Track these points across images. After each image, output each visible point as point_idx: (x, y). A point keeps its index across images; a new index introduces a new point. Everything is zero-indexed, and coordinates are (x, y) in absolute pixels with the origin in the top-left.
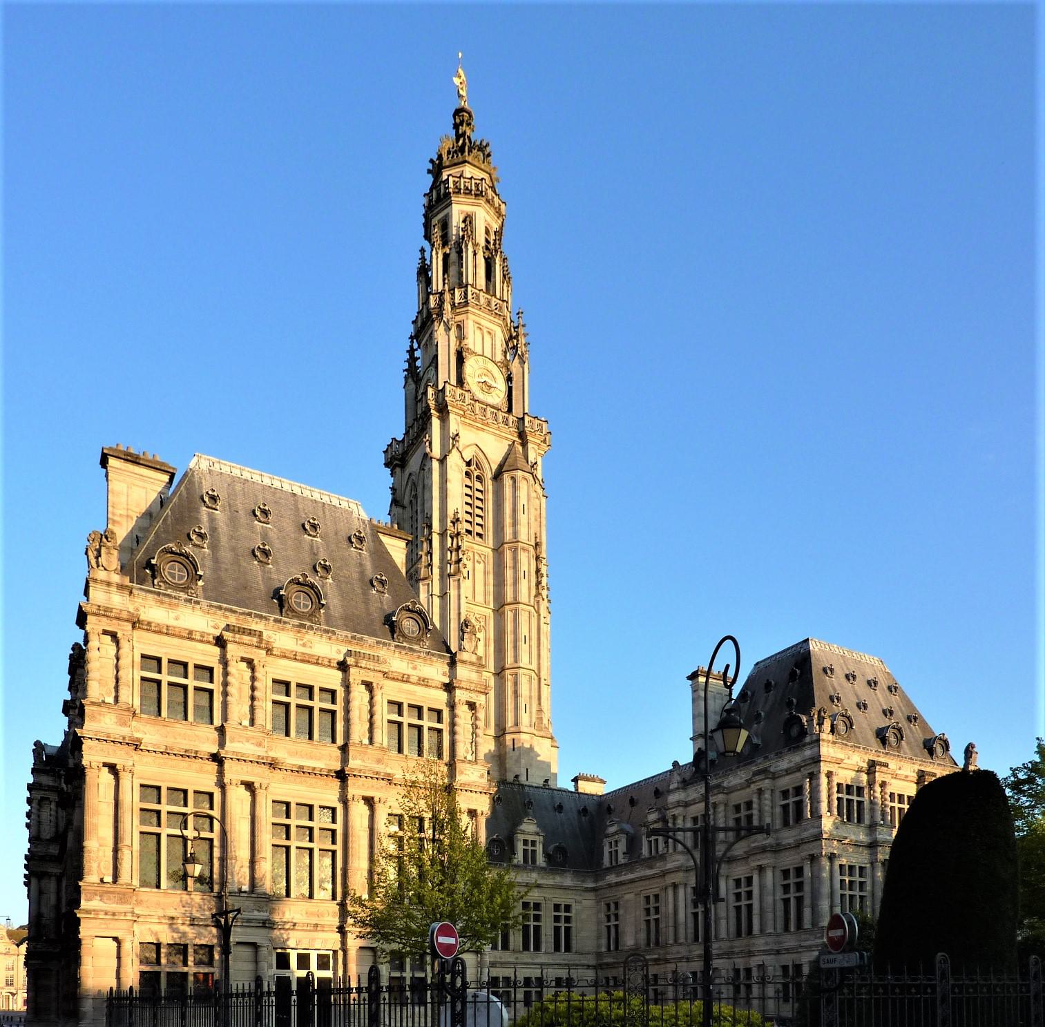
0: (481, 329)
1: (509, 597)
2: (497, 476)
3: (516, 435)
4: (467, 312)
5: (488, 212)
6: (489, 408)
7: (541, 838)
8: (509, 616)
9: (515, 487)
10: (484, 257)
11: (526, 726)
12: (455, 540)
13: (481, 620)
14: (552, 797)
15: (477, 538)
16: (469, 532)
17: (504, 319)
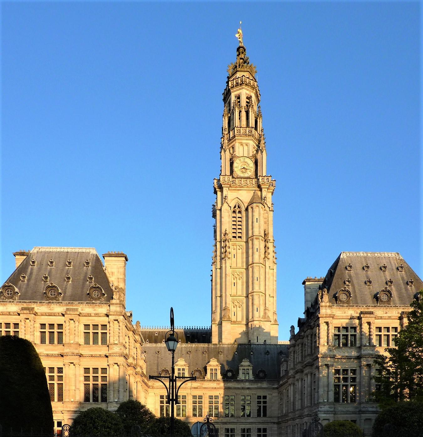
0: (242, 145)
1: (250, 262)
2: (247, 209)
3: (256, 187)
4: (235, 140)
5: (247, 90)
6: (243, 179)
7: (252, 368)
8: (250, 269)
9: (253, 211)
10: (245, 111)
11: (257, 318)
12: (225, 243)
13: (240, 274)
14: (265, 348)
15: (240, 239)
16: (235, 237)
17: (253, 136)
